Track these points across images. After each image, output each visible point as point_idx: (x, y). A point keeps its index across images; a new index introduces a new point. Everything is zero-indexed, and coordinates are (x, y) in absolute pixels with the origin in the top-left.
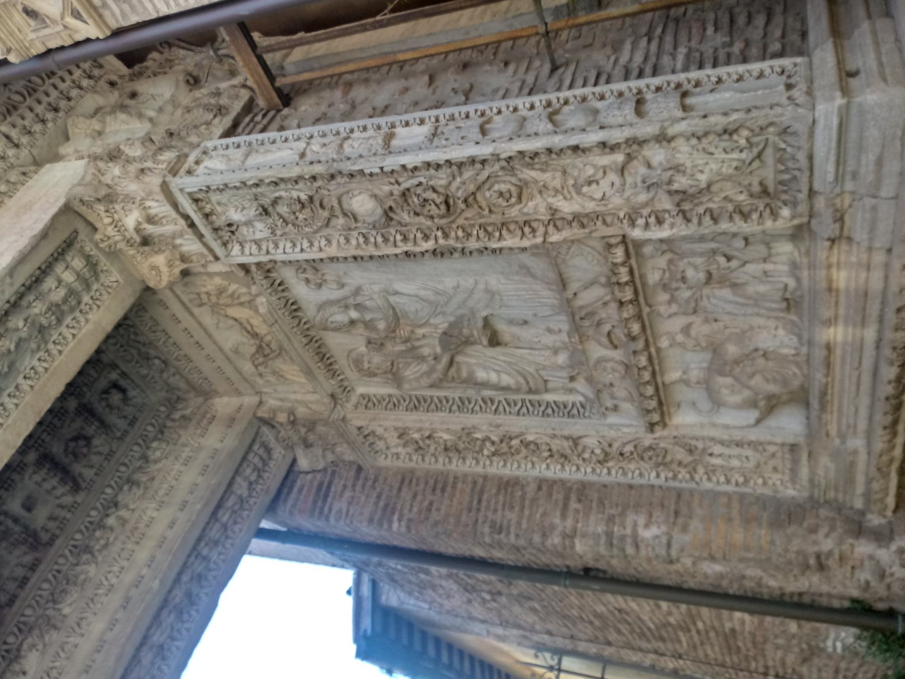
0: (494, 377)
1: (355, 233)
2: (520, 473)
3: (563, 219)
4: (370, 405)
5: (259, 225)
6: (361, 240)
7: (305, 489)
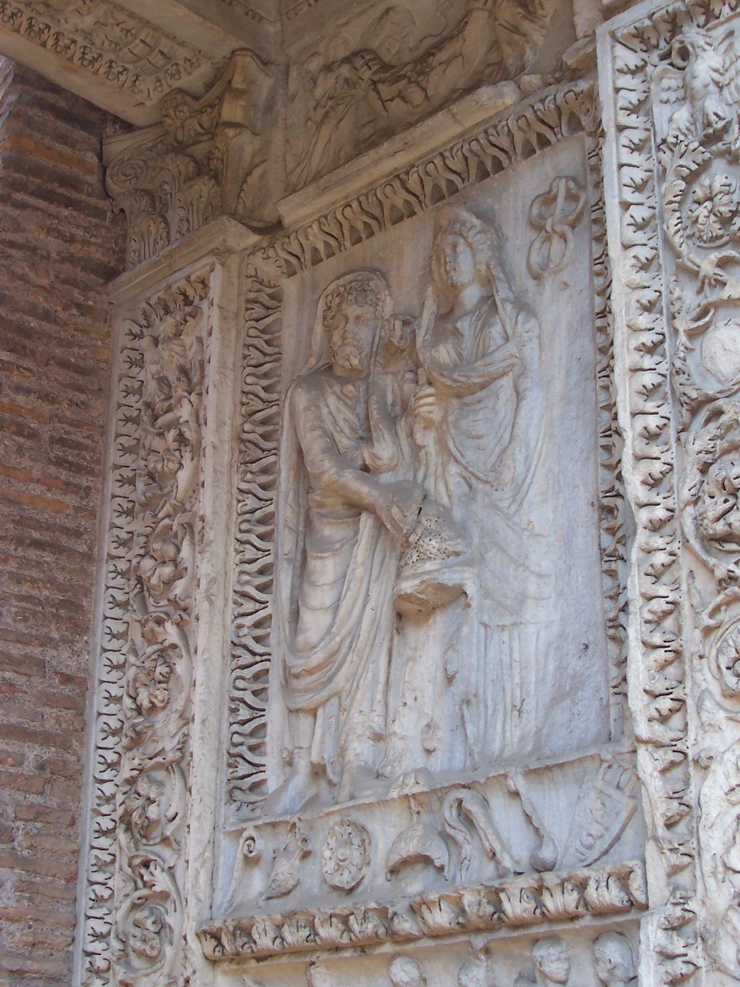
0: (320, 596)
1: (662, 325)
2: (100, 639)
3: (687, 782)
4: (258, 311)
5: (683, 115)
6: (648, 338)
7: (68, 150)
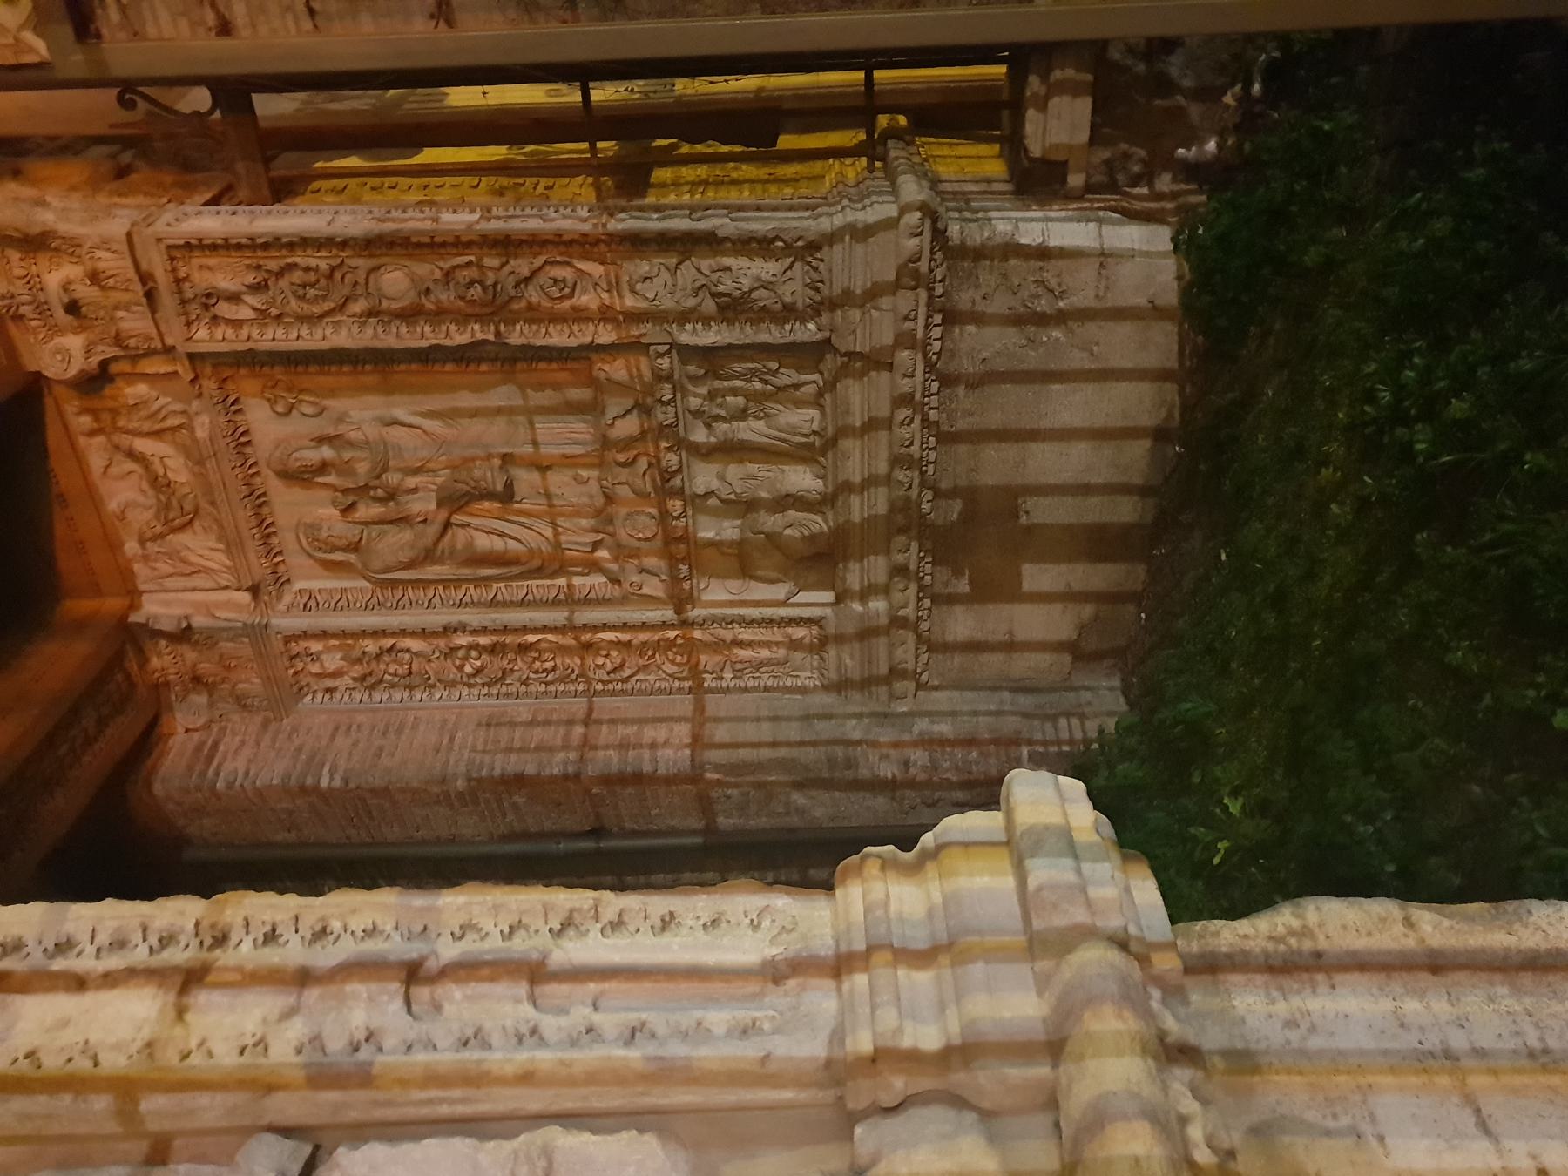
4: (312, 603)
